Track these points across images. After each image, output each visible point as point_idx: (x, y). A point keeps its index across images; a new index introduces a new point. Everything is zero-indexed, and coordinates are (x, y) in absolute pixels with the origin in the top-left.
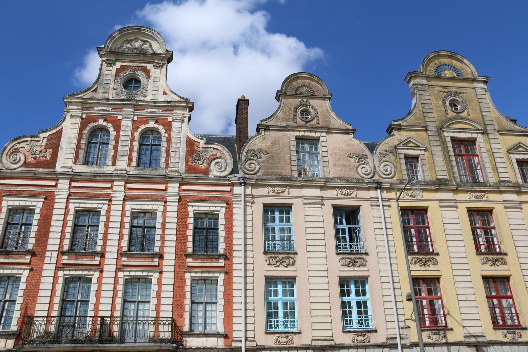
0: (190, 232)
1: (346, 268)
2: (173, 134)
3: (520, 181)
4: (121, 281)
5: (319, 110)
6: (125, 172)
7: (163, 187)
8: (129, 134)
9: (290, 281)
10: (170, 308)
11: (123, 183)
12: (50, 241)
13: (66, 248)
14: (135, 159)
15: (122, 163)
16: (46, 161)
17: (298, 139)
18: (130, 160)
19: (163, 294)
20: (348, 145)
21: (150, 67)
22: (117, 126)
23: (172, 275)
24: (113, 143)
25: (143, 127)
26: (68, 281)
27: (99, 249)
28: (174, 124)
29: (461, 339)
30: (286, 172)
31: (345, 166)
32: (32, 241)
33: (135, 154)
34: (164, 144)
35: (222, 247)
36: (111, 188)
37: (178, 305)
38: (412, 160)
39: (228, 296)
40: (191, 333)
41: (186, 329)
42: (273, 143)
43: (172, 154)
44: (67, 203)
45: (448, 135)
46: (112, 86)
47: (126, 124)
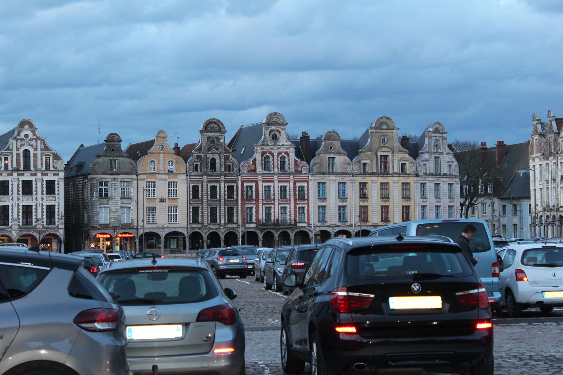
0: (297, 192)
1: (341, 203)
2: (290, 158)
3: (400, 172)
4: (280, 208)
5: (336, 146)
6: (277, 173)
7: (289, 178)
8: (277, 158)
9: (324, 207)
10: (293, 216)
11: (277, 177)
12: (259, 197)
13: (264, 198)
14: (279, 168)
15: (276, 170)
16: (253, 169)
17: (329, 158)
18: (278, 168)
19: (291, 212)
20: (346, 160)
21: (280, 130)
22: (273, 156)
23: (293, 206)
24: (272, 162)
25: (280, 156)
26: (266, 208)
27: (273, 199)
28: (290, 154)
29: (371, 224)
30: (324, 171)
31: (343, 168)
32: (254, 197)
33: (279, 166)
34: (288, 162)
35: (306, 197)
36: (274, 179)
37: (295, 215)
38: (365, 165)
39: (308, 212)
40: (299, 222)
41: (298, 221)
42: (321, 160)
43: (290, 166)
44: (262, 184)
45: (379, 154)
46: (269, 139)
47: (276, 154)
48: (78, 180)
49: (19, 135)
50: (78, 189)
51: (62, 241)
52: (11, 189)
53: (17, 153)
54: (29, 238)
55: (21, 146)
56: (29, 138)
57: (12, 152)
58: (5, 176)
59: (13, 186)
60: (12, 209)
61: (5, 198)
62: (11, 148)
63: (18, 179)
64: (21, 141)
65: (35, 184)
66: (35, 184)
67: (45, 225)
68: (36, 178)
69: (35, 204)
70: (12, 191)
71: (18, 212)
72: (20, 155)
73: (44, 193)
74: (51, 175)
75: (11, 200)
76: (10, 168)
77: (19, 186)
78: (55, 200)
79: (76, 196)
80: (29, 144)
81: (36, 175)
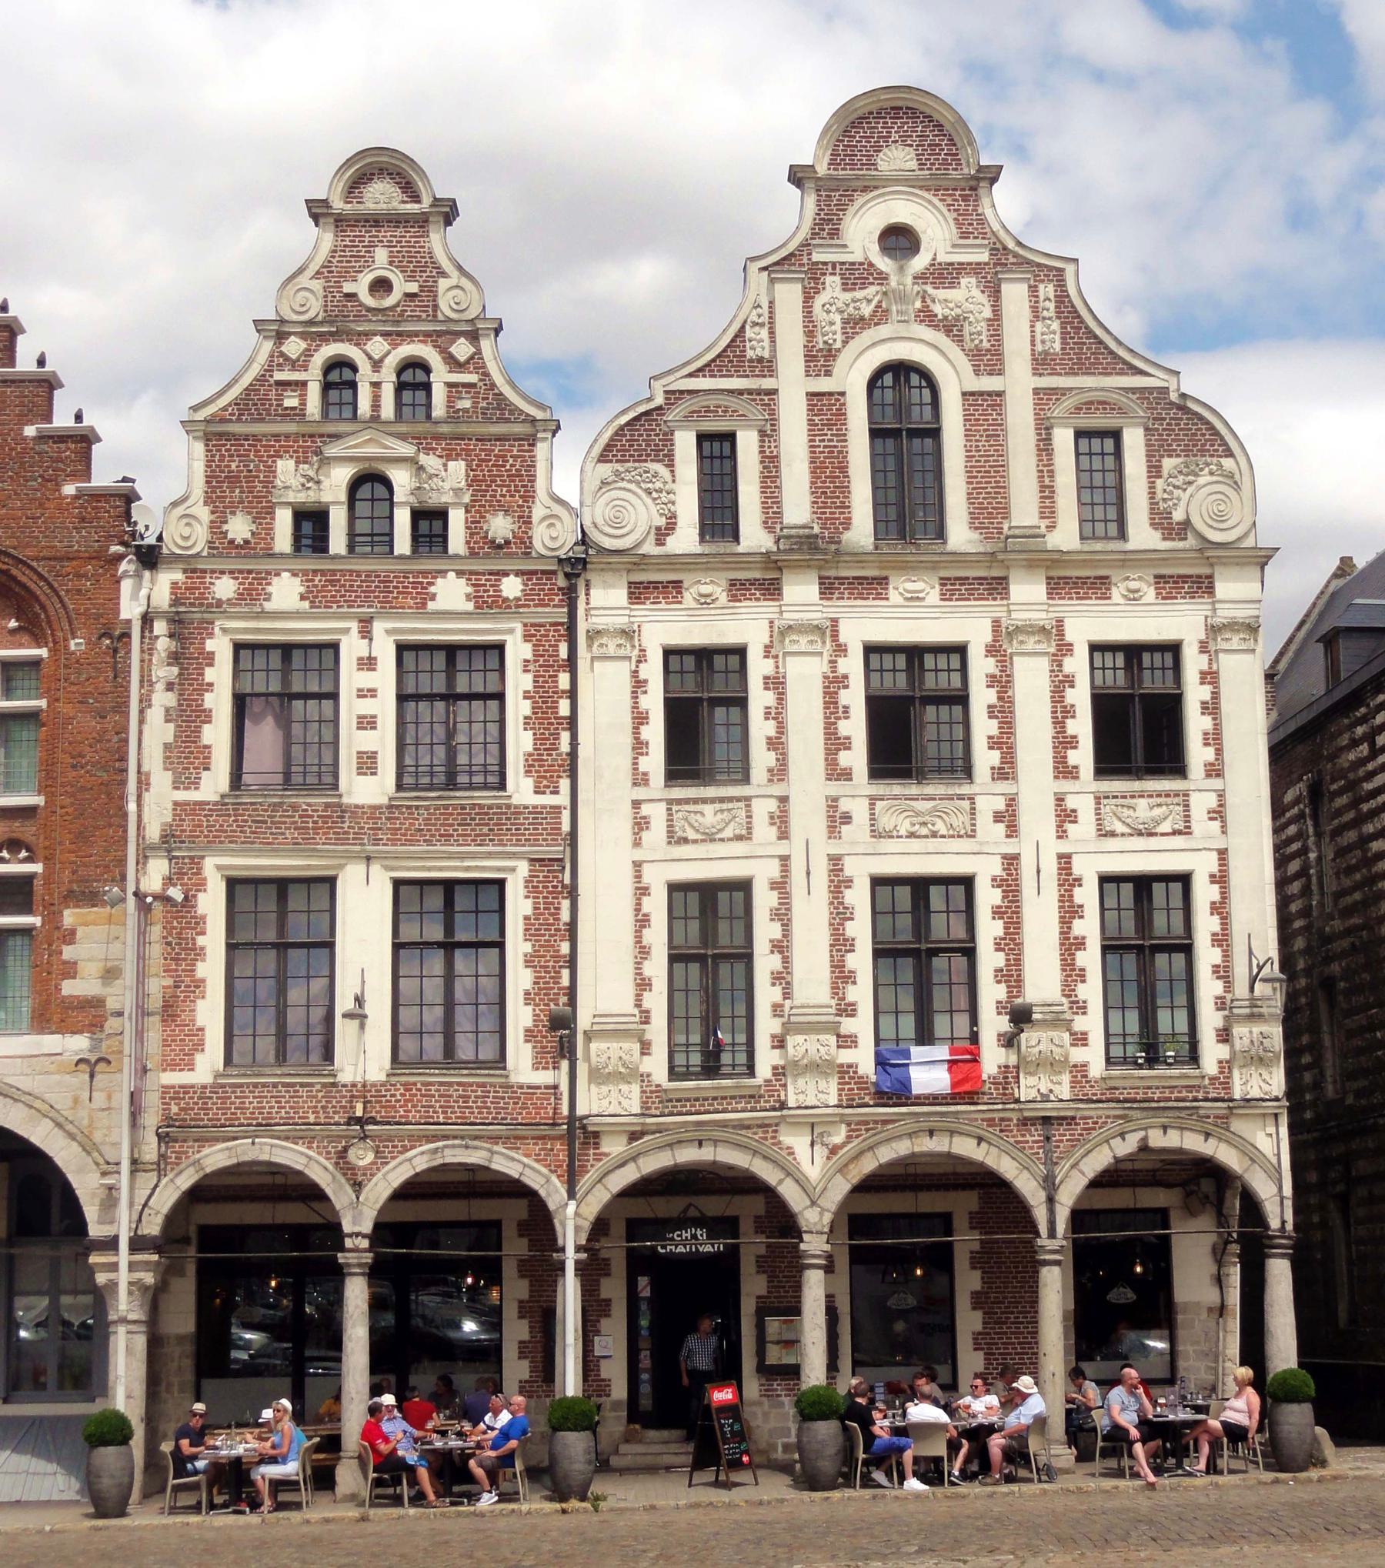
48: (1360, 730)
49: (835, 233)
50: (1365, 807)
51: (1274, 1223)
52: (770, 728)
53: (811, 395)
54: (963, 1204)
55: (855, 325)
56: (919, 262)
57: (767, 383)
58: (706, 600)
59: (781, 698)
60: (782, 915)
61: (709, 815)
62: (757, 345)
63: (831, 630)
64: (846, 288)
65: (992, 681)
66: (992, 681)
67: (1097, 1068)
68: (996, 624)
69: (996, 868)
70: (776, 744)
71: (841, 944)
72: (841, 414)
73: (1073, 757)
74: (1133, 596)
75: (764, 832)
76: (753, 536)
77: (844, 697)
78: (1186, 831)
79: (1350, 870)
80: (927, 317)
81: (997, 587)
